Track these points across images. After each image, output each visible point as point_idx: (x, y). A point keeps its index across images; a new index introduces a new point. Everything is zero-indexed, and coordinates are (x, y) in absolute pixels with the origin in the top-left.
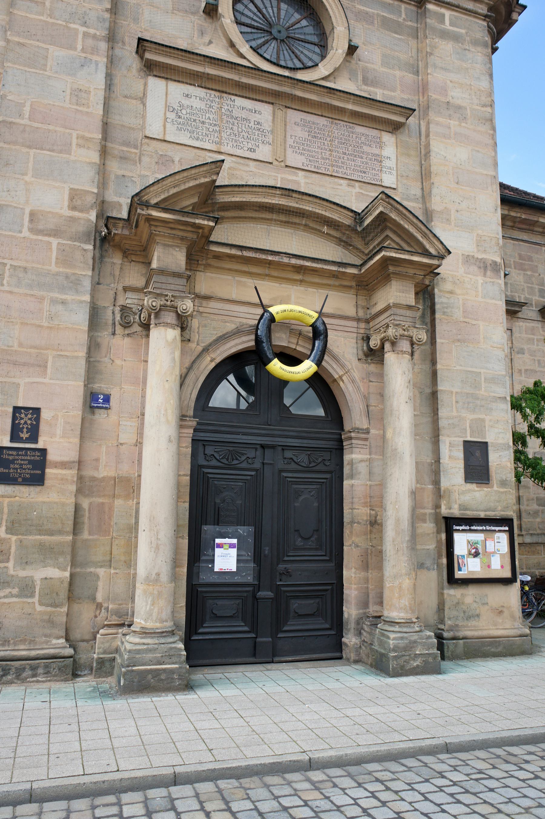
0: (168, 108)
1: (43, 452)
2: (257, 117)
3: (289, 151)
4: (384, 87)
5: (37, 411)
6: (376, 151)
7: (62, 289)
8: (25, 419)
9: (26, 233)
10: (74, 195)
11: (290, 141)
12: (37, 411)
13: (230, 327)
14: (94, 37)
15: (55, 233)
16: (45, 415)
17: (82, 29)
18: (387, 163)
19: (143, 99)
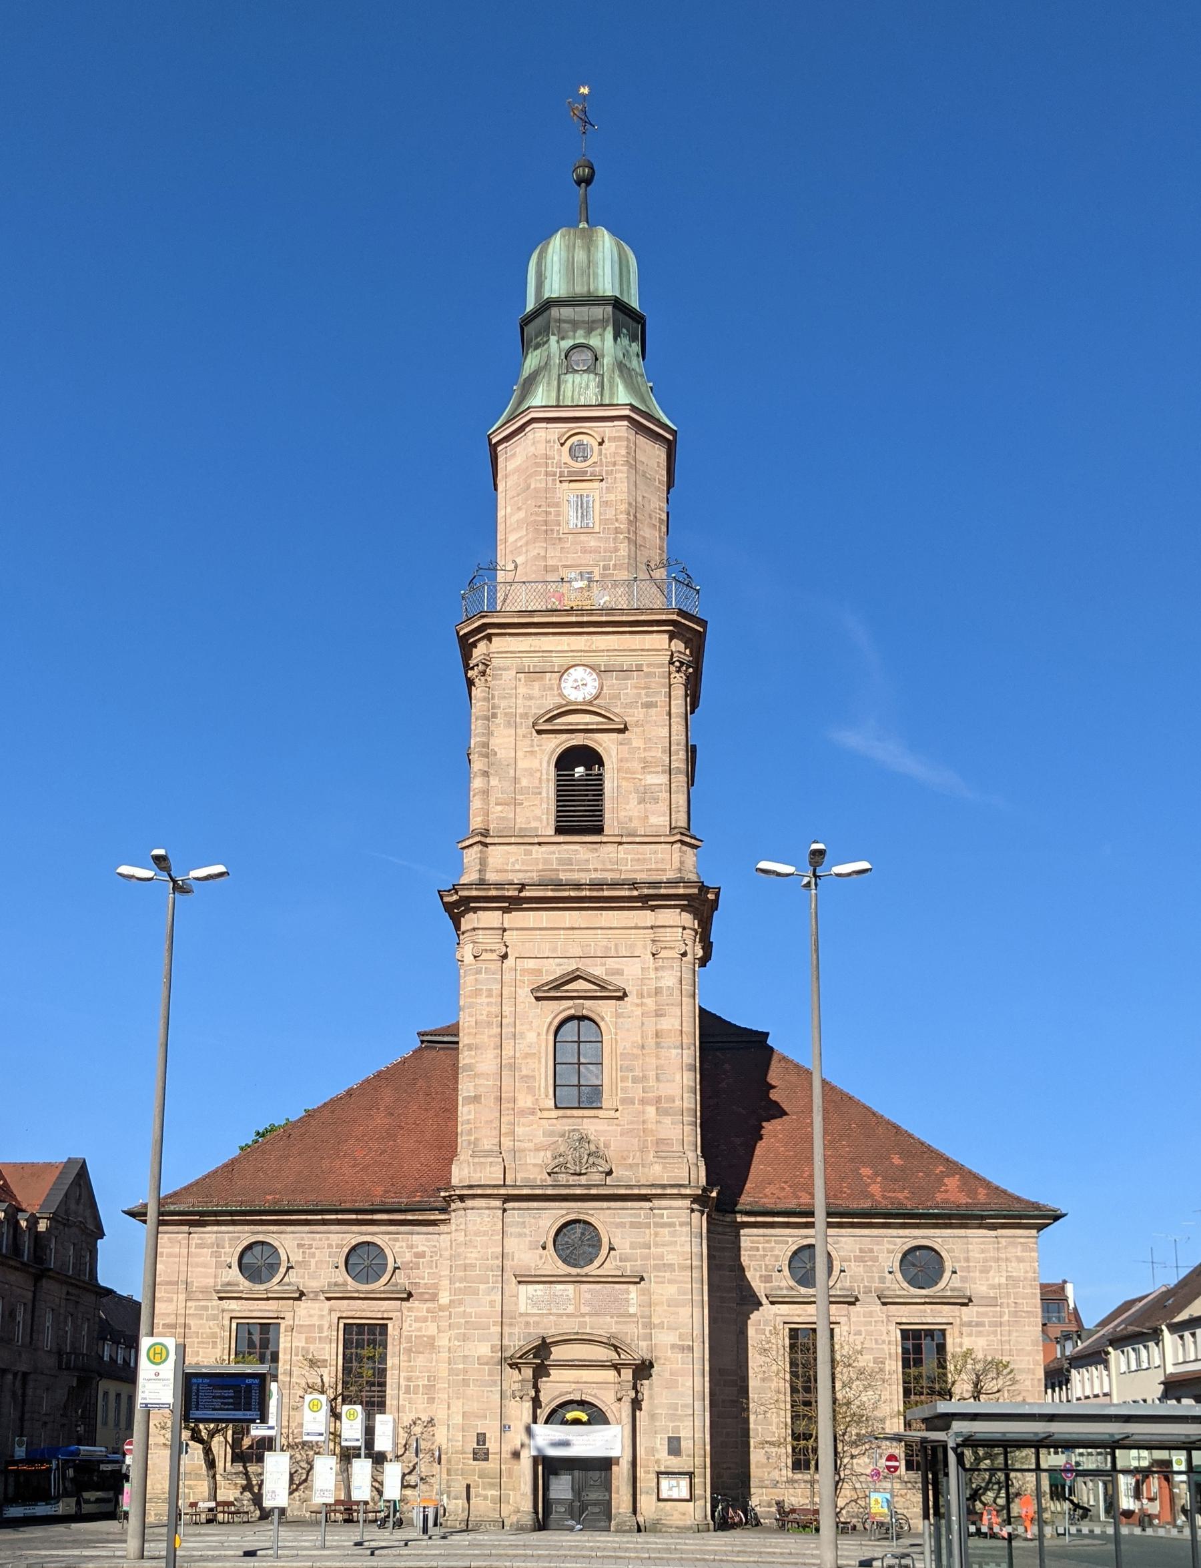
0: (528, 1298)
1: (488, 1449)
2: (567, 1293)
3: (582, 1306)
4: (631, 1261)
5: (485, 1434)
6: (626, 1296)
7: (491, 1386)
8: (481, 1438)
9: (477, 1365)
10: (492, 1346)
11: (582, 1301)
12: (485, 1434)
13: (557, 1393)
14: (497, 1276)
15: (486, 1364)
16: (487, 1436)
17: (491, 1273)
18: (632, 1301)
19: (517, 1296)
